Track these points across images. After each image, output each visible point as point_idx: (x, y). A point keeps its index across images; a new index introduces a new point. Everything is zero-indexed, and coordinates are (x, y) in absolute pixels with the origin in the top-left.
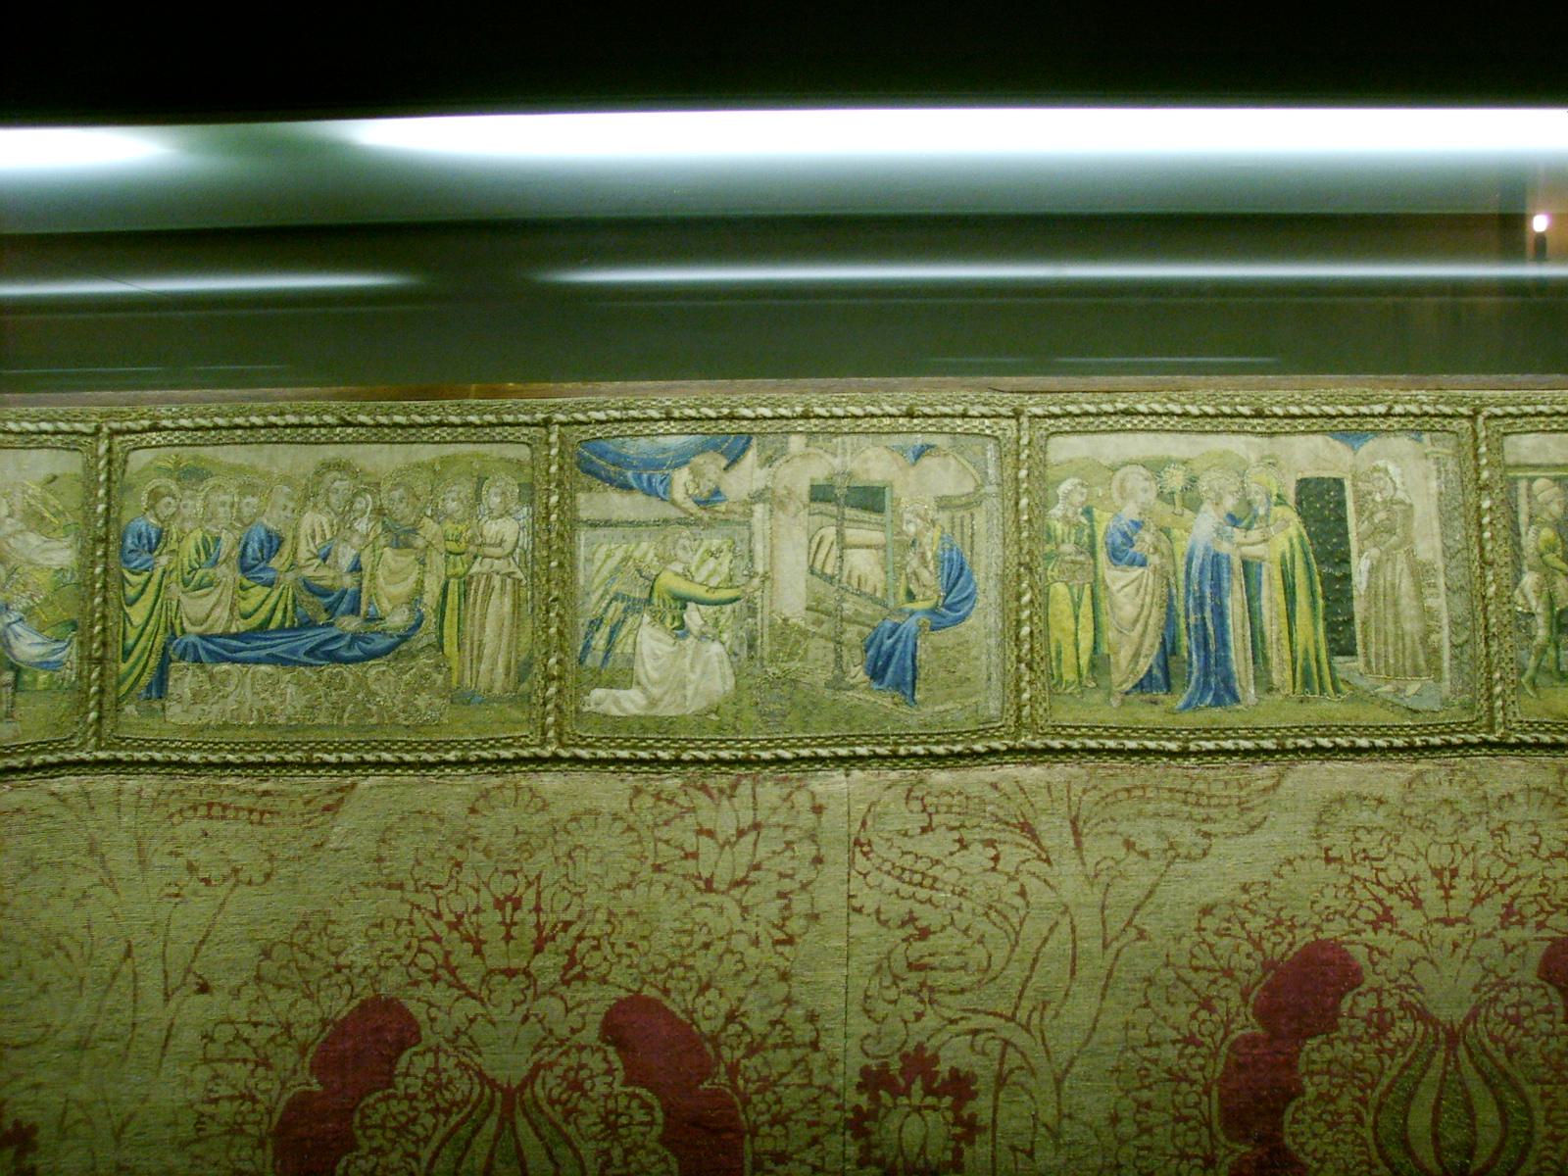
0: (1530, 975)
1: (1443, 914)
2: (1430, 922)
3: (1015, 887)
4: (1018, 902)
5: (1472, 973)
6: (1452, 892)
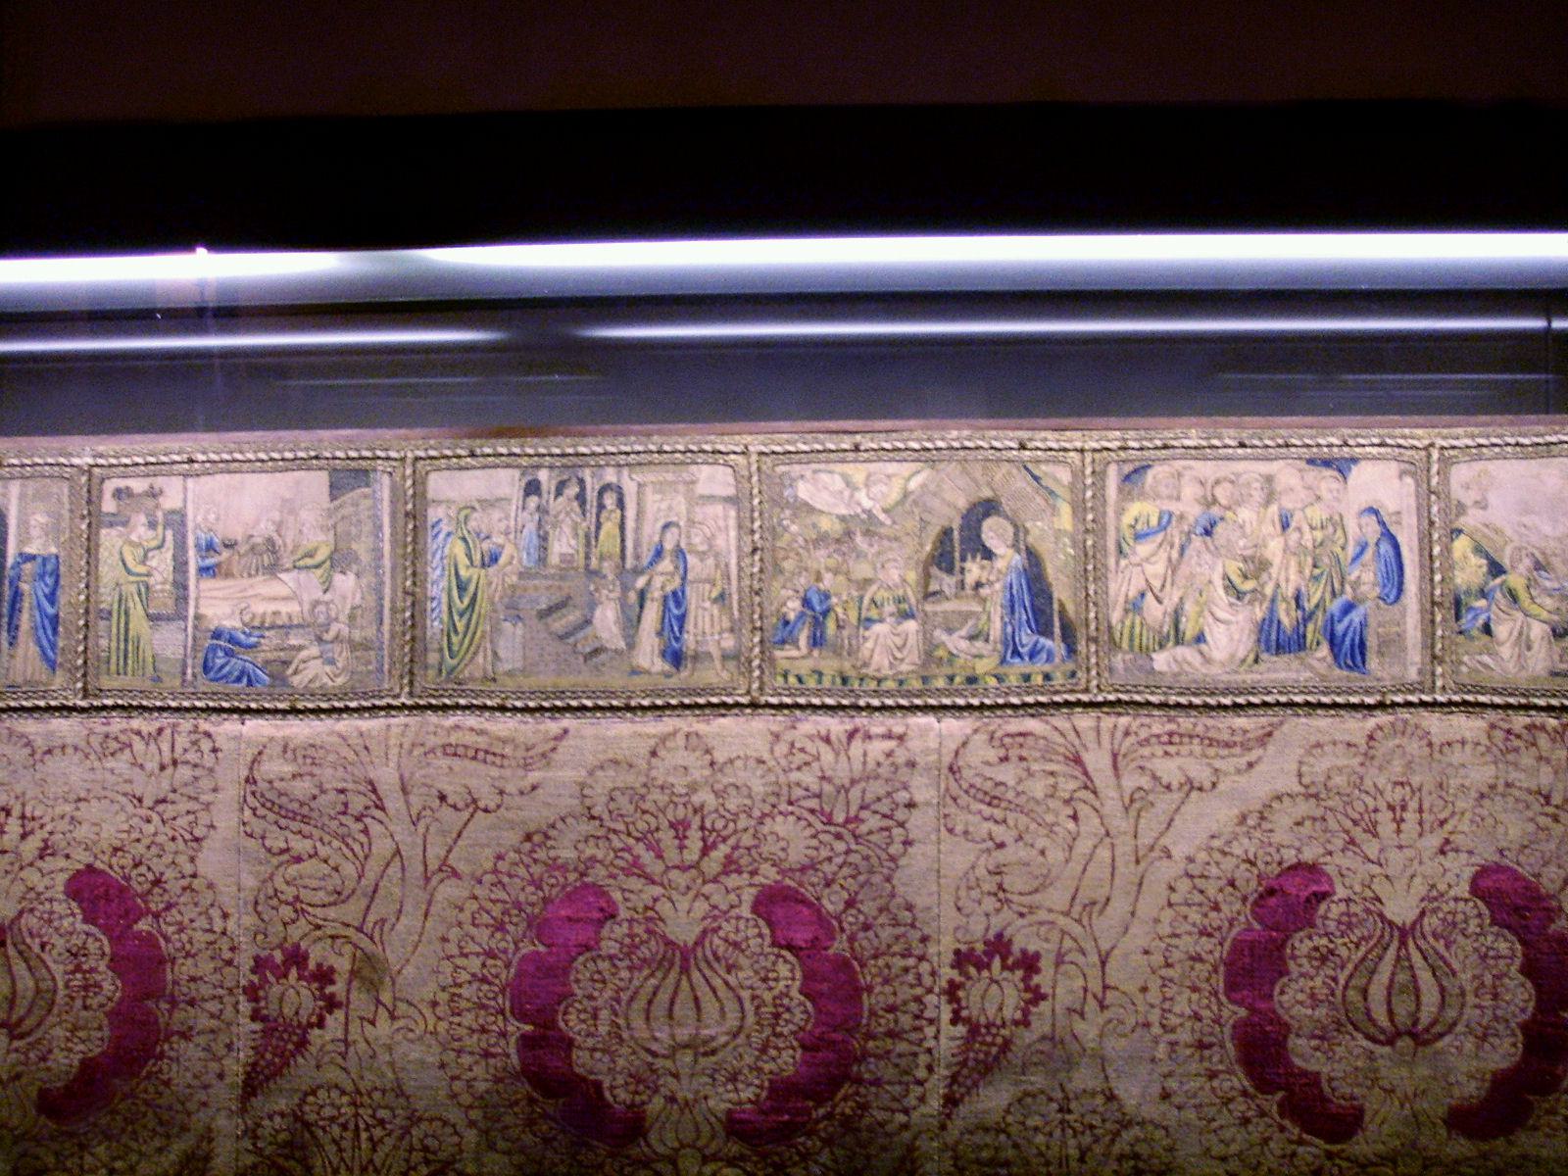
0: (745, 911)
1: (677, 862)
2: (668, 868)
3: (360, 826)
4: (363, 838)
5: (701, 907)
6: (687, 842)
